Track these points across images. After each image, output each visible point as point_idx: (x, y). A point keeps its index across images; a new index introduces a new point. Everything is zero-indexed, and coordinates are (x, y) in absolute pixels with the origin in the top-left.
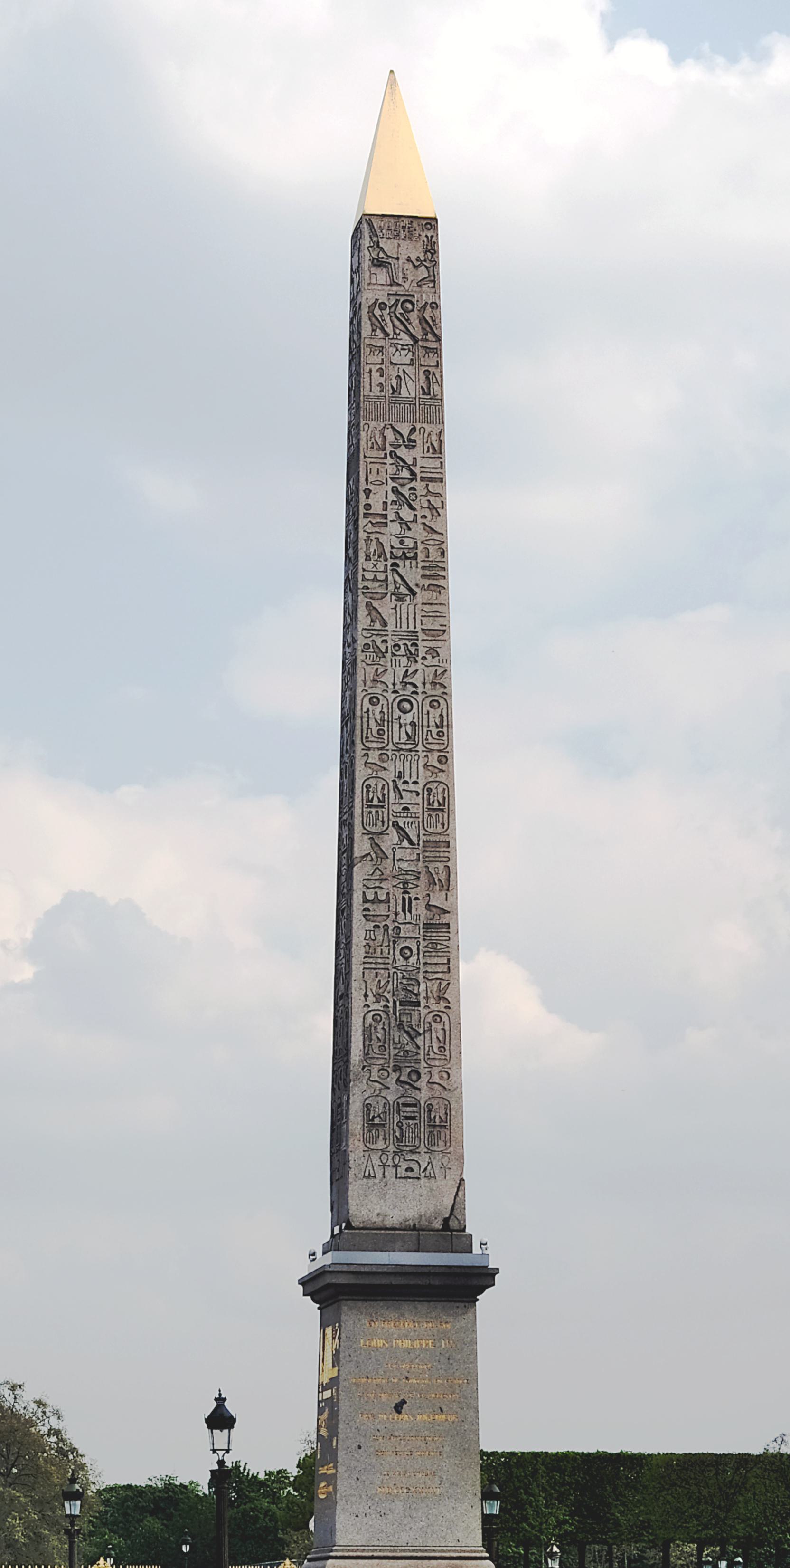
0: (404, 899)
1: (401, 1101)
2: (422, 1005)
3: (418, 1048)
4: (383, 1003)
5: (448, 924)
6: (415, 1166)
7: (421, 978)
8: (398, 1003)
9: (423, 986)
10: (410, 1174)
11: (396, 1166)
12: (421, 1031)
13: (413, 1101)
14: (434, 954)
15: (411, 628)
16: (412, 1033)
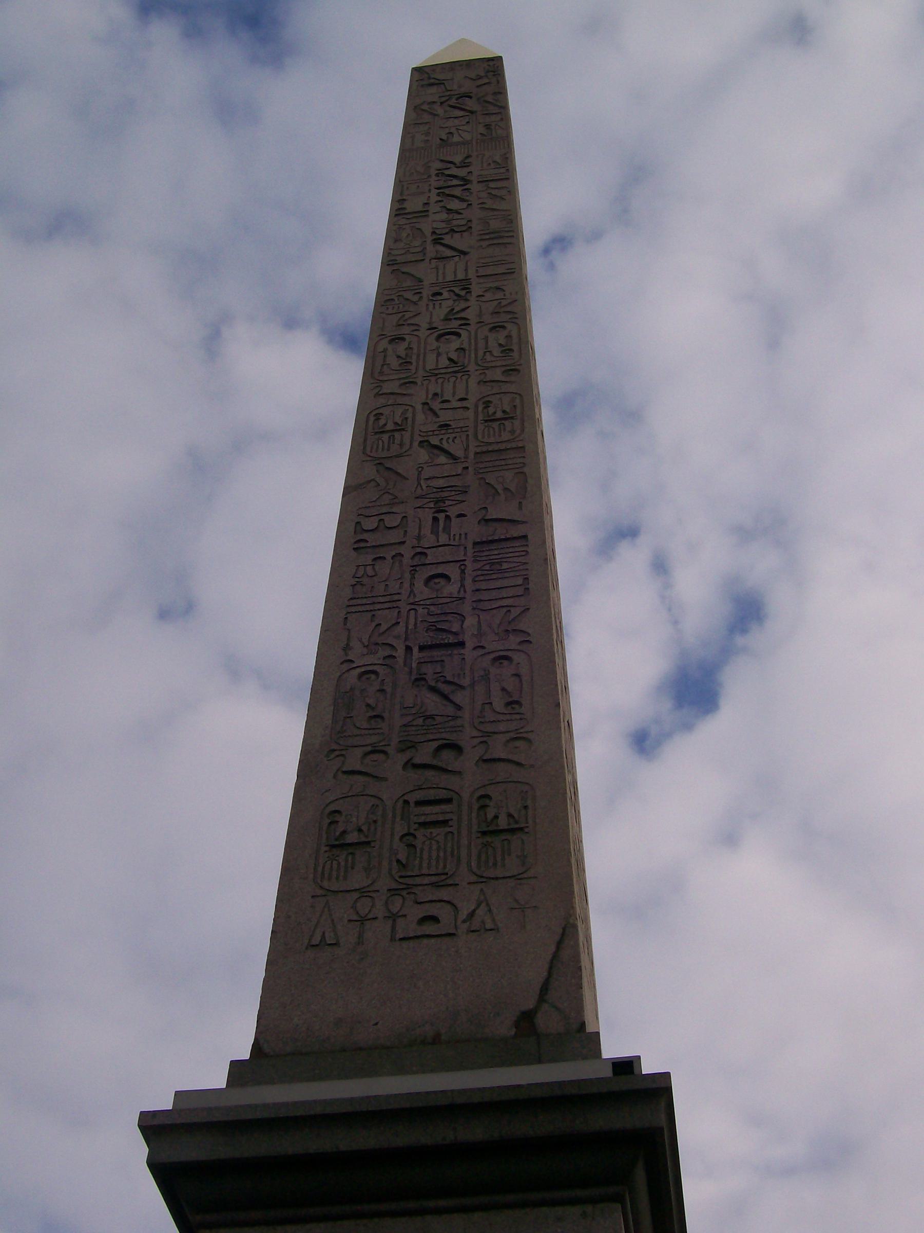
0: (435, 519)
1: (413, 798)
2: (469, 644)
3: (459, 708)
4: (383, 652)
5: (525, 537)
6: (443, 912)
7: (466, 608)
8: (416, 650)
9: (470, 621)
10: (429, 929)
11: (393, 917)
12: (466, 682)
13: (443, 794)
14: (494, 576)
15: (461, 276)
16: (445, 689)
